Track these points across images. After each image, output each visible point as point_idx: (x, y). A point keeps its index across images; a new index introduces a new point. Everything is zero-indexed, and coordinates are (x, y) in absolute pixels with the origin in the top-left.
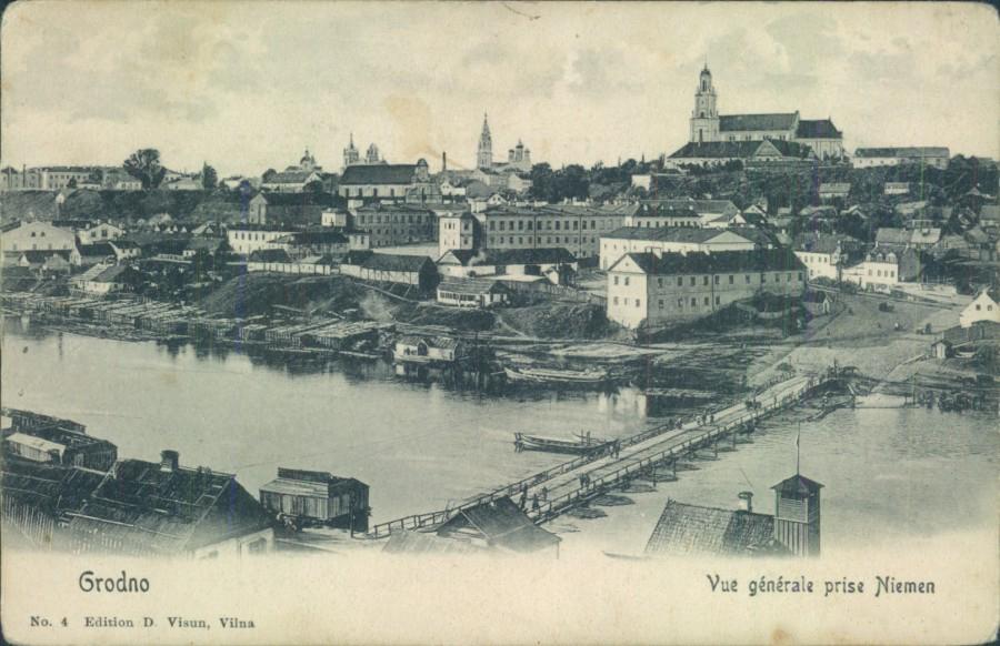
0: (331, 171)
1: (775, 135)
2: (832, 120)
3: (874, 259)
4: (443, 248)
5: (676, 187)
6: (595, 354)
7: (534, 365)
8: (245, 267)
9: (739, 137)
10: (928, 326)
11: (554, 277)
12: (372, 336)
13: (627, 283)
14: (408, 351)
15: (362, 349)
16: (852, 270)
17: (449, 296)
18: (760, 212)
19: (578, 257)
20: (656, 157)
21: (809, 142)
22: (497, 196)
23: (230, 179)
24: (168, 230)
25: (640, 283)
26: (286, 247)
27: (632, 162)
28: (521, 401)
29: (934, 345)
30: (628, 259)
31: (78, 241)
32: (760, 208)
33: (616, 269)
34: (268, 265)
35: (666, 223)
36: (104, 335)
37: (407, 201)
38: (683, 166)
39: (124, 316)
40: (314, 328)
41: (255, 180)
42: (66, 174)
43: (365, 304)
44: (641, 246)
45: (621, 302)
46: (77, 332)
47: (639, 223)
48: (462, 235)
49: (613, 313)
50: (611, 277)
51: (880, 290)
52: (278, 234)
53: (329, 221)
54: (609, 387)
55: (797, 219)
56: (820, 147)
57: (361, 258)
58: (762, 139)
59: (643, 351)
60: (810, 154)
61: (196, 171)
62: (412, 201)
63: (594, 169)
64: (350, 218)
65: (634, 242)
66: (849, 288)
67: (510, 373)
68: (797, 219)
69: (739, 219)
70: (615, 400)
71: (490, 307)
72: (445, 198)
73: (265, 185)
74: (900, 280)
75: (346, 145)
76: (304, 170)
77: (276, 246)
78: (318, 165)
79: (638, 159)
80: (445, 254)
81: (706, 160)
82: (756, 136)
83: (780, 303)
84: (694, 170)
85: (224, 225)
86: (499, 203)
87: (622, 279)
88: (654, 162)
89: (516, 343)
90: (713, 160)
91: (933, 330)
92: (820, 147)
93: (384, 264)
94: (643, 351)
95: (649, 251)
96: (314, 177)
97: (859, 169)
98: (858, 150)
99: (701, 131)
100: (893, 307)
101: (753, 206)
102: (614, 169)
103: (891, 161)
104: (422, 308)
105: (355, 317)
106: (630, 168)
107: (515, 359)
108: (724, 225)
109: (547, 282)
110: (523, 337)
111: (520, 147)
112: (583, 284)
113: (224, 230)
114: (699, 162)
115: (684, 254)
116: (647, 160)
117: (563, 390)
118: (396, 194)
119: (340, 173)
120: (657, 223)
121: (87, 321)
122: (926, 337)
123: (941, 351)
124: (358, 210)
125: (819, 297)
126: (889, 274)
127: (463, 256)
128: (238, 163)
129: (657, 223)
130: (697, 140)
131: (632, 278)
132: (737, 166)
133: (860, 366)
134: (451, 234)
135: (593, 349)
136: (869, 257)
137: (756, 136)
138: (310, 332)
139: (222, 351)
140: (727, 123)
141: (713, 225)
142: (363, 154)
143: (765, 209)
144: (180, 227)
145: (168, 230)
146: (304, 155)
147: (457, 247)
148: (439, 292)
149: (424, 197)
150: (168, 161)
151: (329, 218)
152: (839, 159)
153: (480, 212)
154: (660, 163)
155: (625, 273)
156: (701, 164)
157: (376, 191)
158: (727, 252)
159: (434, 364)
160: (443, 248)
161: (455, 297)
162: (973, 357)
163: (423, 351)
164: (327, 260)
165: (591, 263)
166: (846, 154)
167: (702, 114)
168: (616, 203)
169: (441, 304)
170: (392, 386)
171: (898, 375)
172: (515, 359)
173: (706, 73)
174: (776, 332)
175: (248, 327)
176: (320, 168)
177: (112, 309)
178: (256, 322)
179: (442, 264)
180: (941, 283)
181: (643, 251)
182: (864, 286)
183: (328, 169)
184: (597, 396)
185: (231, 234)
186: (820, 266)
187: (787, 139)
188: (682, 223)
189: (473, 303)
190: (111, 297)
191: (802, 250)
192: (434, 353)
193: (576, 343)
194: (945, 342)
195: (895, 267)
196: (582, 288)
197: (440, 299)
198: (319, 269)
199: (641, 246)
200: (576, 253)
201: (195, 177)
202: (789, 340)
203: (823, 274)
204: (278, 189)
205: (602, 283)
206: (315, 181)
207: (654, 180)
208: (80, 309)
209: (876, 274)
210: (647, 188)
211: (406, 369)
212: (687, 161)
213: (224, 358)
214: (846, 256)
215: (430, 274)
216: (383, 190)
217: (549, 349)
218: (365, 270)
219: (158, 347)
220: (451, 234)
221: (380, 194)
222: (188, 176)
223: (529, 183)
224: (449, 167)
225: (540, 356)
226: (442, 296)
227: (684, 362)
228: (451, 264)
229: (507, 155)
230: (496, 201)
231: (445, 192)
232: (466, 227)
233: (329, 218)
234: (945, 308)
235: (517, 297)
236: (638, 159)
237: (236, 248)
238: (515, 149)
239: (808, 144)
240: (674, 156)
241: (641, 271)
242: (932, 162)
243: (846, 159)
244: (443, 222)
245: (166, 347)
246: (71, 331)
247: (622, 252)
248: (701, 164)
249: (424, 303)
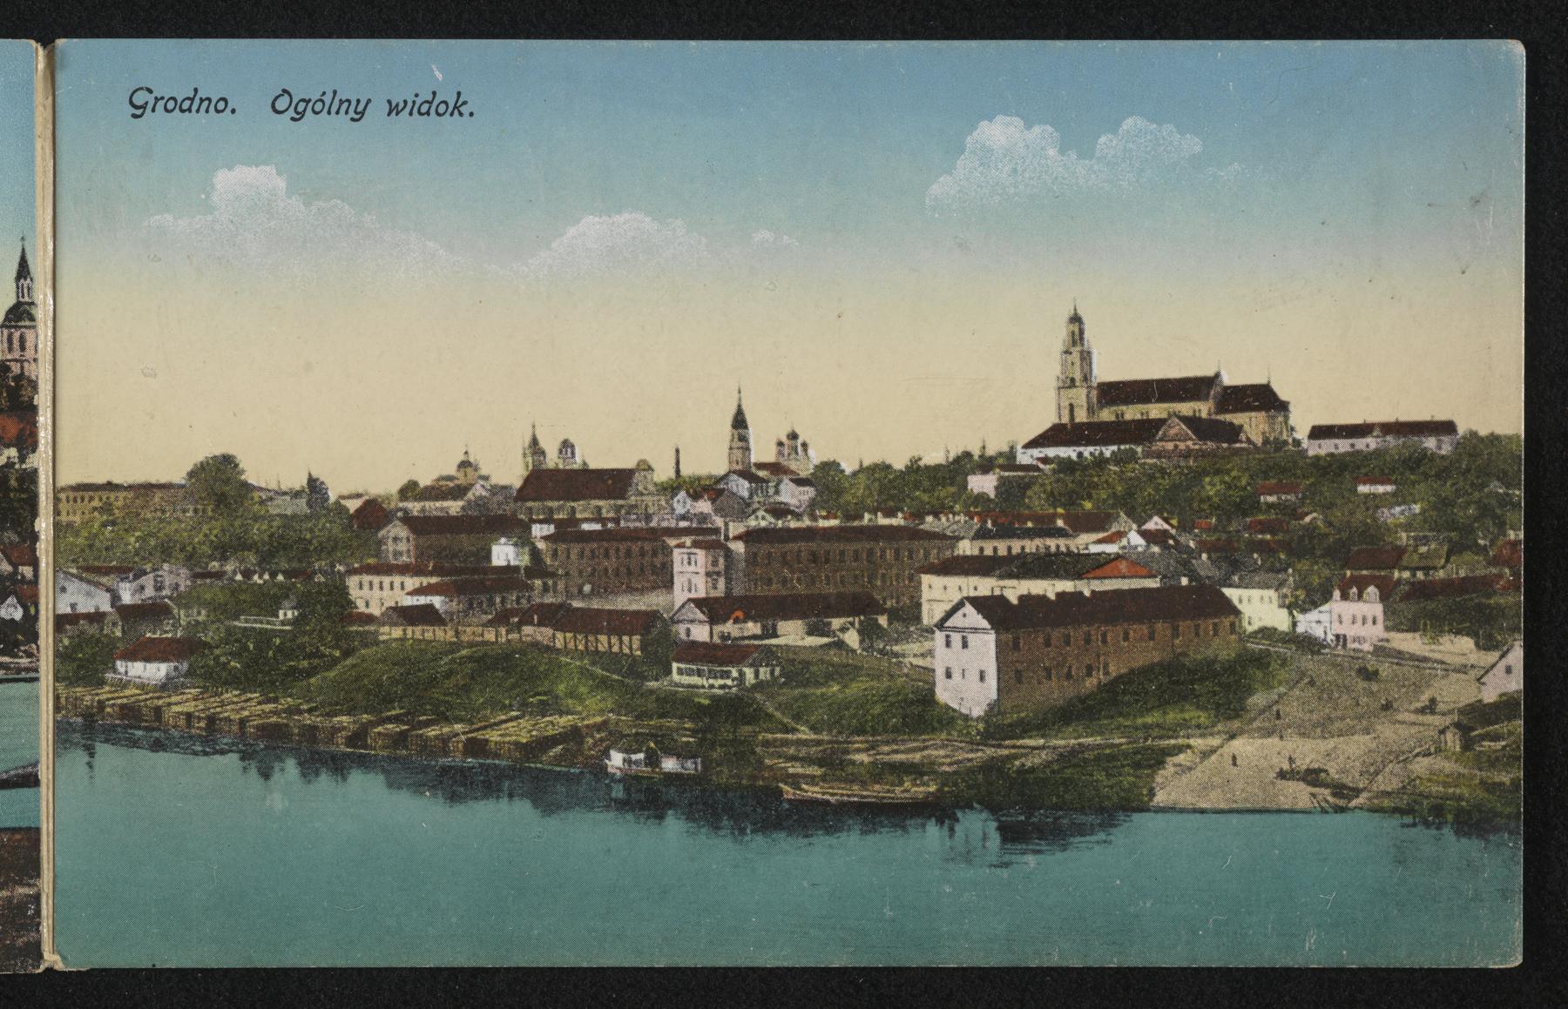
0: (503, 482)
2: (1276, 387)
3: (1345, 597)
4: (680, 595)
5: (1028, 500)
6: (917, 757)
7: (824, 778)
8: (377, 632)
9: (1132, 412)
10: (1433, 701)
11: (852, 638)
12: (574, 735)
13: (965, 645)
14: (627, 761)
15: (558, 760)
16: (1313, 615)
17: (690, 673)
18: (1166, 526)
19: (889, 604)
20: (1006, 449)
21: (1238, 418)
22: (761, 513)
23: (350, 497)
24: (256, 577)
25: (985, 646)
26: (437, 601)
27: (968, 455)
28: (806, 836)
29: (1442, 732)
30: (968, 608)
31: (115, 598)
32: (1166, 520)
33: (948, 624)
34: (409, 630)
35: (1023, 548)
36: (157, 746)
37: (622, 524)
38: (1045, 460)
39: (189, 716)
40: (485, 728)
41: (388, 498)
42: (96, 495)
43: (561, 688)
44: (985, 586)
45: (956, 675)
46: (115, 742)
47: (982, 549)
48: (708, 574)
49: (944, 694)
50: (939, 636)
51: (1356, 645)
52: (426, 581)
53: (503, 557)
54: (940, 810)
55: (1224, 536)
56: (1253, 425)
57: (555, 616)
58: (1164, 416)
59: (990, 752)
60: (1243, 437)
61: (298, 488)
62: (631, 525)
64: (535, 554)
65: (974, 580)
66: (1309, 644)
67: (788, 791)
68: (1224, 536)
69: (1136, 539)
70: (952, 830)
71: (754, 687)
72: (683, 517)
73: (400, 505)
74: (1387, 629)
75: (528, 439)
76: (462, 481)
77: (422, 600)
78: (483, 472)
79: (976, 453)
80: (683, 606)
81: (1081, 449)
82: (1156, 411)
83: (1209, 671)
84: (1066, 466)
85: (340, 568)
86: (763, 524)
87: (956, 638)
88: (1001, 454)
89: (799, 742)
90: (1091, 449)
91: (1441, 707)
93: (588, 622)
94: (990, 752)
95: (997, 592)
96: (478, 491)
97: (1317, 458)
99: (1071, 406)
100: (1376, 673)
101: (1156, 519)
102: (938, 467)
104: (652, 692)
105: (543, 709)
106: (962, 465)
107: (796, 769)
109: (840, 645)
110: (805, 733)
111: (793, 436)
112: (896, 648)
113: (342, 576)
114: (1069, 452)
115: (1052, 596)
116: (991, 452)
117: (876, 815)
118: (604, 515)
119: (518, 484)
120: (1009, 549)
121: (138, 725)
122: (1429, 719)
123: (1452, 741)
124: (545, 538)
125: (1261, 661)
126: (1370, 621)
127: (714, 609)
128: (364, 471)
129: (1009, 549)
130: (1065, 420)
131: (971, 638)
132: (1132, 456)
133: (1332, 771)
134: (692, 575)
135: (914, 750)
136: (1337, 594)
137: (1156, 411)
138: (479, 735)
139: (339, 766)
140: (1114, 393)
141: (1094, 549)
143: (1174, 522)
144: (273, 575)
145: (256, 577)
146: (462, 458)
147: (702, 594)
148: (675, 665)
150: (256, 472)
151: (503, 553)
152: (1285, 443)
153: (738, 538)
154: (1011, 455)
155: (962, 630)
156: (1074, 456)
158: (1115, 592)
159: (671, 778)
160: (680, 595)
161: (699, 673)
162: (1504, 747)
163: (653, 760)
164: (502, 619)
165: (908, 614)
166: (1298, 436)
167: (1073, 380)
168: (944, 519)
169: (677, 685)
170: (602, 816)
171: (1388, 781)
172: (796, 769)
174: (1203, 717)
175: (380, 729)
176: (486, 478)
177: (169, 704)
178: (396, 719)
179: (679, 622)
180: (1450, 631)
181: (988, 593)
182: (1330, 637)
183: (499, 479)
184: (924, 826)
185: (352, 582)
186: (1259, 607)
187: (1204, 415)
188: (1048, 548)
189: (729, 682)
190: (166, 686)
191: (1238, 587)
192: (669, 764)
193: (887, 743)
194: (1457, 725)
195: (1377, 609)
196: (896, 655)
197: (676, 677)
198: (490, 636)
199: (985, 586)
200: (884, 600)
201: (296, 494)
202: (1220, 727)
203: (1268, 623)
204: (423, 510)
205: (927, 645)
206: (481, 497)
207: (1003, 482)
208: (122, 707)
209: (1352, 619)
210: (992, 496)
211: (627, 790)
212: (1051, 452)
213: (344, 779)
214: (1301, 594)
216: (582, 508)
217: (847, 752)
218: (559, 635)
219: (241, 764)
220: (692, 575)
221: (579, 516)
222: (285, 493)
223: (809, 493)
224: (686, 471)
225: (833, 763)
226: (680, 672)
227: (1056, 767)
228: (692, 621)
229: (774, 449)
230: (762, 520)
231: (680, 510)
232: (715, 563)
233: (503, 553)
234: (1459, 671)
235: (796, 669)
236: (976, 453)
237: (361, 604)
238: (784, 440)
239: (1236, 422)
241: (985, 624)
243: (1297, 443)
244: (678, 556)
245: (253, 765)
246: (107, 741)
247: (957, 598)
248: (1074, 456)
249: (652, 684)
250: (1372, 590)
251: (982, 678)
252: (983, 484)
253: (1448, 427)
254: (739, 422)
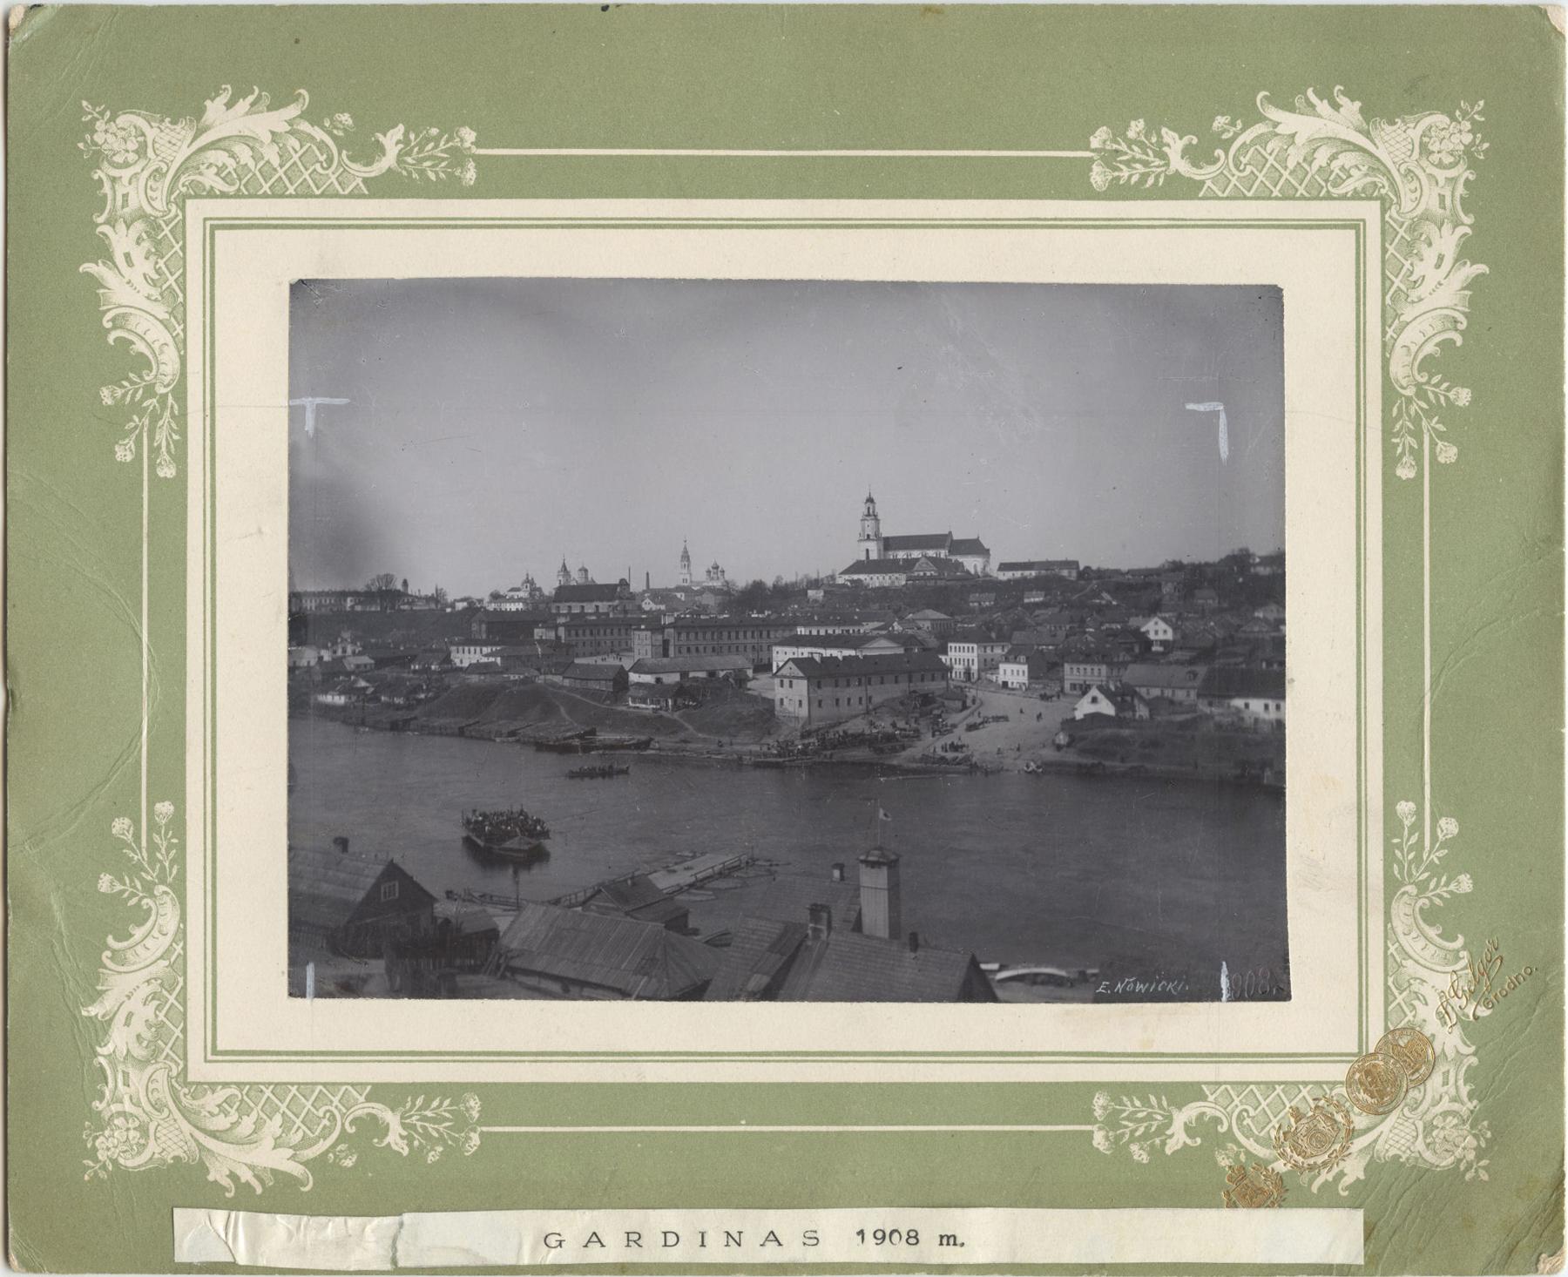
1: (931, 553)
9: (901, 555)
25: (802, 686)
30: (791, 664)
44: (805, 652)
65: (801, 650)
77: (492, 659)
82: (916, 554)
87: (786, 681)
92: (972, 563)
130: (863, 558)
131: (795, 681)
137: (916, 554)
140: (889, 544)
149: (626, 612)
173: (870, 500)
199: (805, 652)
215: (620, 681)
237: (457, 661)
240: (846, 572)
242: (1065, 573)
253: (1072, 565)
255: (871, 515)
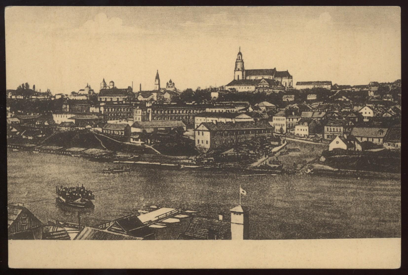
1: (266, 77)
2: (289, 72)
9: (253, 78)
13: (203, 134)
25: (207, 135)
56: (285, 81)
63: (197, 90)
65: (208, 118)
78: (92, 89)
82: (260, 78)
87: (201, 132)
98: (298, 82)
103: (311, 87)
108: (245, 111)
137: (260, 78)
142: (108, 84)
157: (111, 99)
173: (240, 53)
188: (228, 111)
207: (220, 95)
216: (115, 99)
221: (113, 100)
224: (142, 90)
240: (228, 85)
241: (208, 130)
242: (325, 87)
250: (306, 124)
251: (207, 143)
252: (215, 95)
253: (329, 83)
254: (157, 77)
255: (240, 59)
